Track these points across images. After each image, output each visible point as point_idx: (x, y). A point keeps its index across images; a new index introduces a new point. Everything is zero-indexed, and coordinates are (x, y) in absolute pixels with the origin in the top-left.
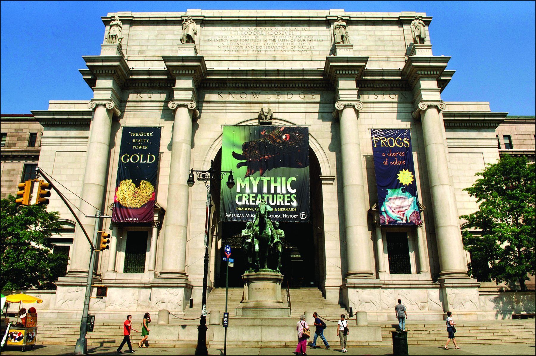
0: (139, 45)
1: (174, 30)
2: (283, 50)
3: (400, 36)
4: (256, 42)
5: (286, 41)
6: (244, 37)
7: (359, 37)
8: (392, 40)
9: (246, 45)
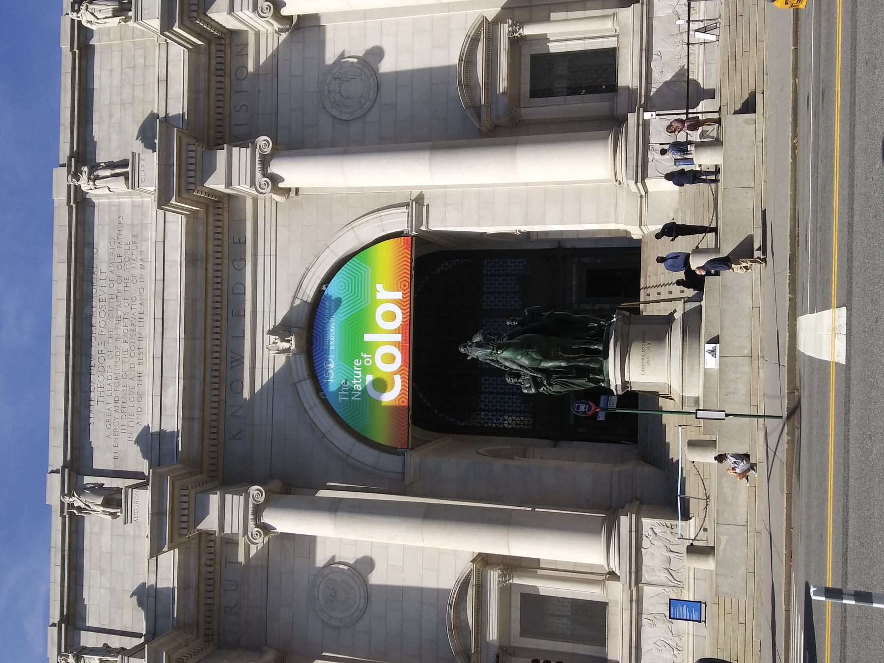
0: (122, 609)
1: (91, 533)
2: (139, 301)
5: (119, 295)
6: (109, 382)
7: (114, 137)
8: (122, 69)
9: (127, 379)
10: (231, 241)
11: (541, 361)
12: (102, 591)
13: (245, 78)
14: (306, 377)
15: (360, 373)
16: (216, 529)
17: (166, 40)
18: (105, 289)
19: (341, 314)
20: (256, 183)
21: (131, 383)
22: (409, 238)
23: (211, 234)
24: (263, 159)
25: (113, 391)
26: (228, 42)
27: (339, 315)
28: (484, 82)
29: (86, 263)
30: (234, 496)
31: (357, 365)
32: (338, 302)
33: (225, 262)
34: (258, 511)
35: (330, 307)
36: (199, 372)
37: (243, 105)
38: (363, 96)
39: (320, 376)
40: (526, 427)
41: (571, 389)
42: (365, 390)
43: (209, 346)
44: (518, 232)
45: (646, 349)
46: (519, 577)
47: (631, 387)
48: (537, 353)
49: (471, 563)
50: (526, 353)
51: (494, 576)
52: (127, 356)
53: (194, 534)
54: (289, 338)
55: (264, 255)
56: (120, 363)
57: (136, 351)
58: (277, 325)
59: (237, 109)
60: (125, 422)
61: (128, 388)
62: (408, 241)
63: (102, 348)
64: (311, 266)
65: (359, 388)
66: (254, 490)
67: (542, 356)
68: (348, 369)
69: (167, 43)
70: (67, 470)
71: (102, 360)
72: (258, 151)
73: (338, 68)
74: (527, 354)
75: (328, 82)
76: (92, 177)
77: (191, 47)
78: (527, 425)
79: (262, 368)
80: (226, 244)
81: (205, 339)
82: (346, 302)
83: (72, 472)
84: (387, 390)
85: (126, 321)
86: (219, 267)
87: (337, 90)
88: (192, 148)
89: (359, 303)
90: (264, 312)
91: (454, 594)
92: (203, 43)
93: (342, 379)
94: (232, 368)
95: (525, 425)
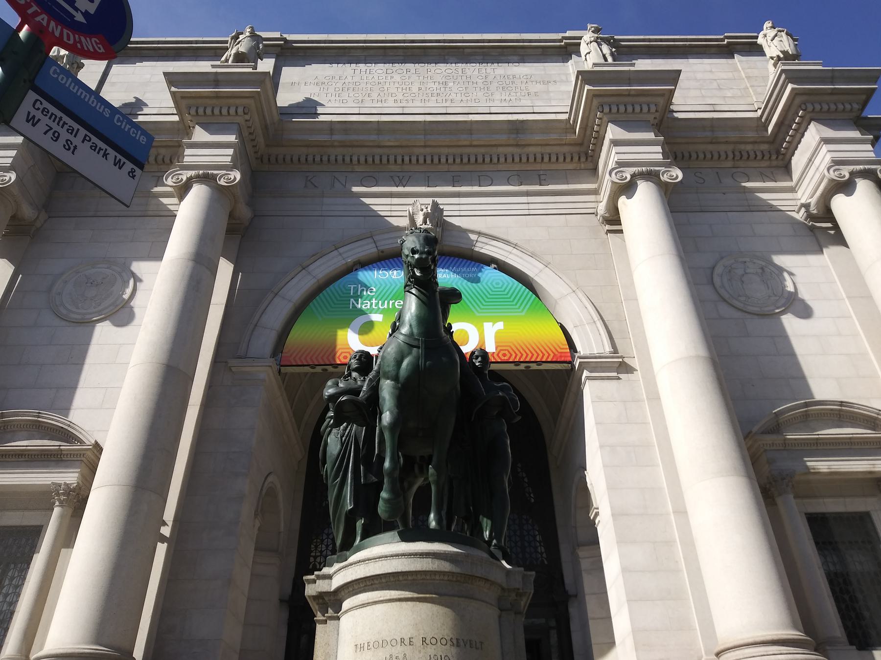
2: (464, 98)
3: (732, 72)
4: (402, 86)
8: (715, 80)
10: (541, 172)
11: (396, 378)
12: (148, 76)
13: (734, 179)
14: (381, 248)
15: (386, 306)
16: (192, 140)
17: (760, 109)
18: (476, 72)
19: (461, 284)
20: (622, 169)
21: (375, 95)
22: (569, 359)
23: (548, 149)
24: (653, 174)
25: (365, 81)
26: (775, 163)
27: (460, 282)
28: (820, 436)
29: (503, 58)
30: (231, 157)
31: (396, 303)
32: (477, 280)
33: (517, 167)
34: (206, 179)
35: (469, 273)
36: (387, 140)
37: (704, 182)
38: (749, 298)
39: (382, 264)
40: (312, 559)
41: (330, 481)
42: (362, 313)
43: (417, 151)
44: (595, 511)
45: (431, 650)
46: (62, 517)
47: (325, 622)
48: (415, 369)
49: (93, 442)
50: (415, 343)
51: (70, 477)
52: (404, 91)
53: (191, 124)
54: (428, 223)
55: (528, 203)
56: (397, 85)
57: (409, 98)
58: (444, 218)
59: (698, 174)
60: (331, 90)
61: (369, 92)
62: (566, 357)
63: (413, 71)
64: (520, 249)
65: (365, 306)
66: (236, 175)
67: (409, 379)
68: (391, 292)
69: (756, 111)
70: (283, 42)
71: (401, 71)
72: (663, 169)
73: (777, 272)
74: (411, 346)
75: (755, 261)
76: (599, 40)
77: (763, 120)
78: (315, 561)
79: (391, 205)
80: (538, 167)
81: (425, 146)
82: (476, 287)
83: (280, 48)
84: (361, 337)
85: (443, 89)
86: (510, 159)
87: (748, 271)
88: (653, 109)
89: (476, 303)
90: (459, 204)
91: (52, 420)
92: (743, 184)
93: (377, 288)
94: (392, 177)
95: (315, 557)
